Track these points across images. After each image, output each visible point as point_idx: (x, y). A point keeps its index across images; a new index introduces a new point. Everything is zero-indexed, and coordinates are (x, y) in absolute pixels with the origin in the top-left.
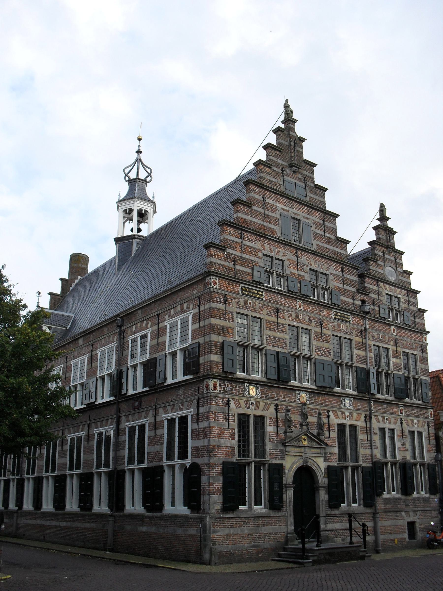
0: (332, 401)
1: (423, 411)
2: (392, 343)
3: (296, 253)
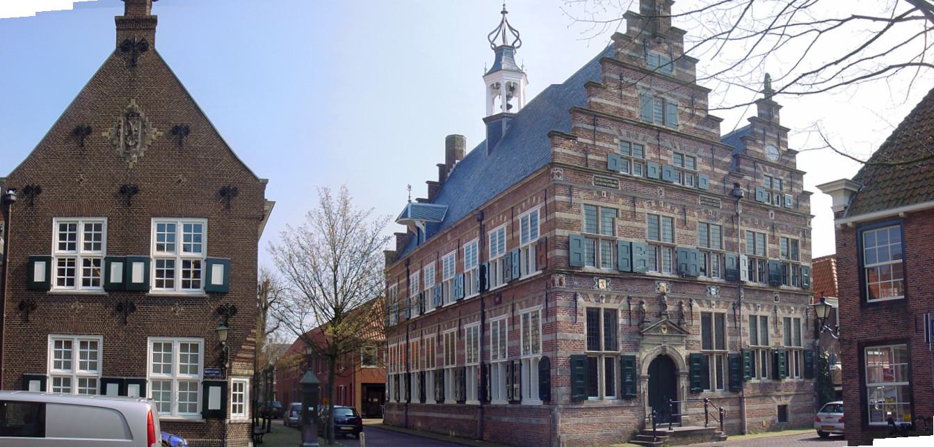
0: (696, 290)
1: (803, 298)
2: (768, 228)
3: (658, 136)
